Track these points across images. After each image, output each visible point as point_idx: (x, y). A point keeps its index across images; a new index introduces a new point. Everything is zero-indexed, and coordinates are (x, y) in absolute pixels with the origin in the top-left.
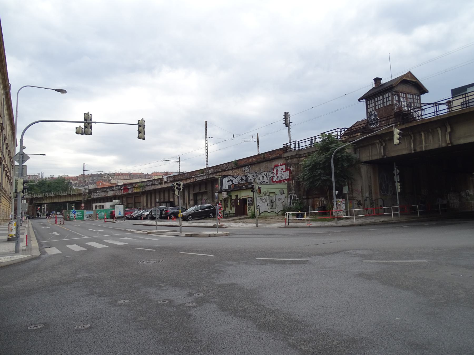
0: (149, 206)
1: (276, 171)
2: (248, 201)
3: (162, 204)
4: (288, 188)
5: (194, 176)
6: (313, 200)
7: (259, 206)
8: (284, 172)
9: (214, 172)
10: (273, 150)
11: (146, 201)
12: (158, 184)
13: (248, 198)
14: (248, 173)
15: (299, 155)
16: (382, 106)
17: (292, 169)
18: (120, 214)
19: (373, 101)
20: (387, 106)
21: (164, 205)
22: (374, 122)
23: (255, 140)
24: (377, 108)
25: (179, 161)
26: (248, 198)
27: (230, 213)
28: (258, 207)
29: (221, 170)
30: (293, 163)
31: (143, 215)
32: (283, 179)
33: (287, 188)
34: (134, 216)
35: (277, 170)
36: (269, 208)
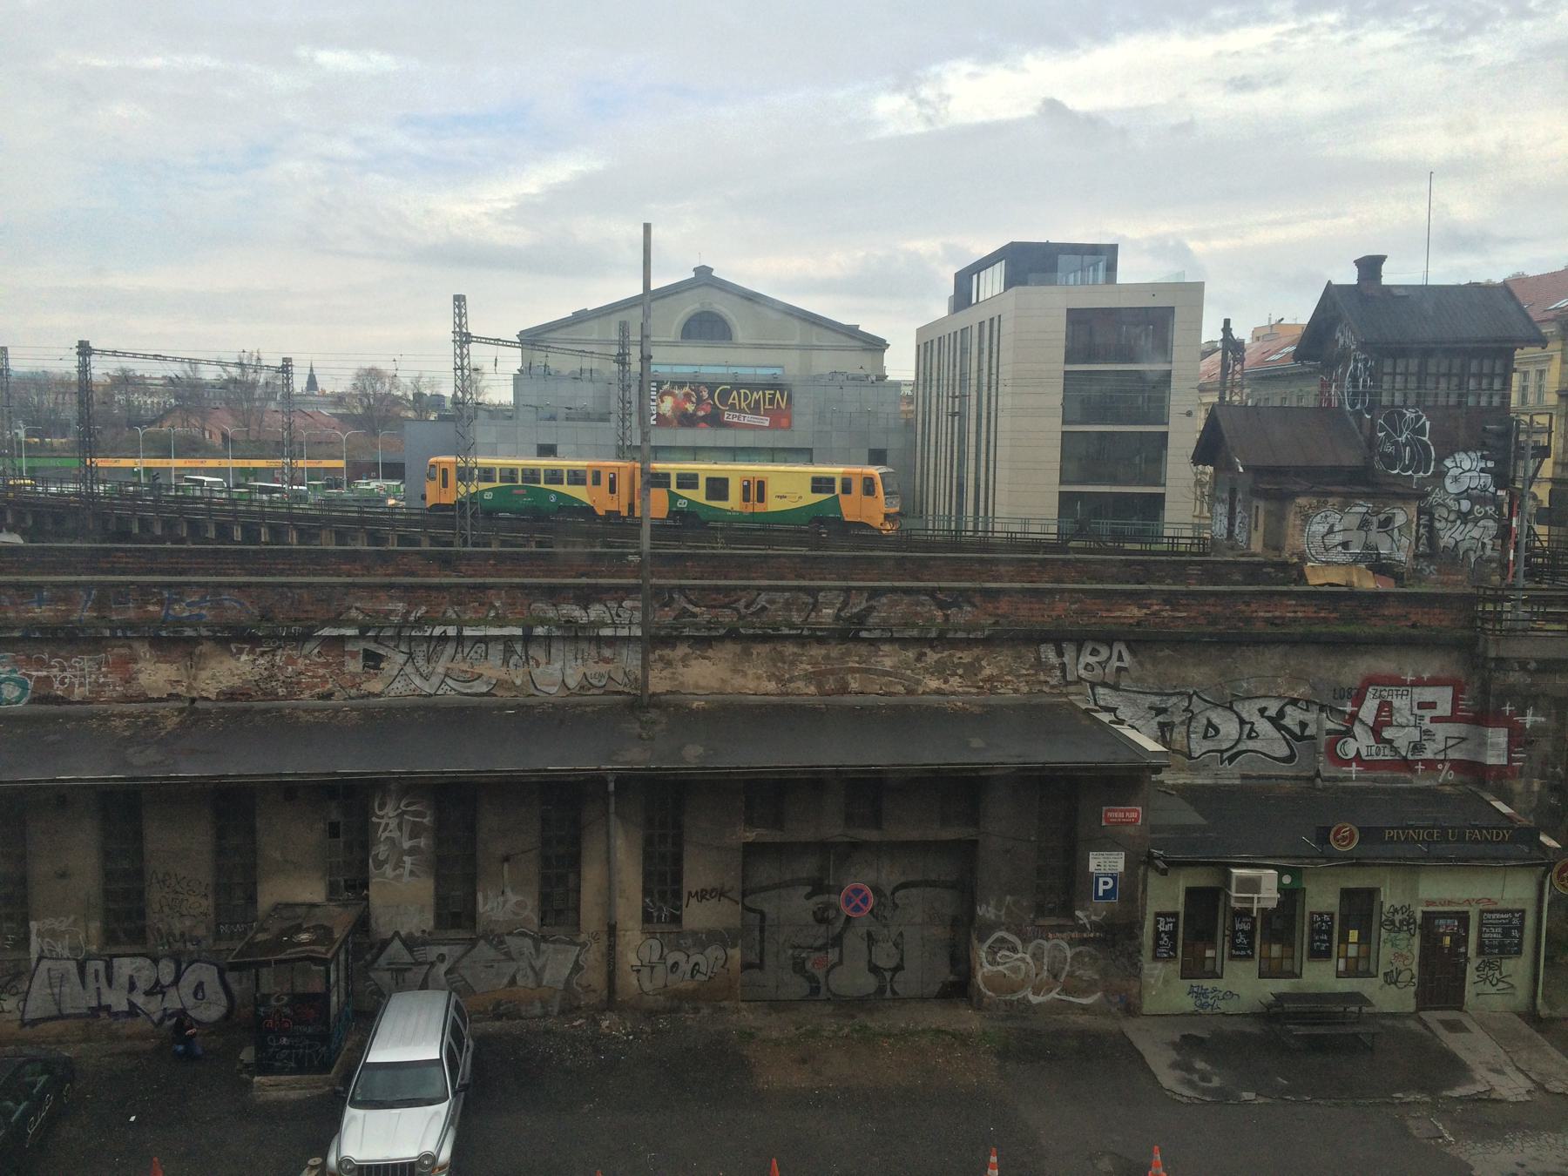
1: (1380, 709)
8: (1434, 720)
13: (1482, 912)
26: (1482, 912)
32: (1428, 755)
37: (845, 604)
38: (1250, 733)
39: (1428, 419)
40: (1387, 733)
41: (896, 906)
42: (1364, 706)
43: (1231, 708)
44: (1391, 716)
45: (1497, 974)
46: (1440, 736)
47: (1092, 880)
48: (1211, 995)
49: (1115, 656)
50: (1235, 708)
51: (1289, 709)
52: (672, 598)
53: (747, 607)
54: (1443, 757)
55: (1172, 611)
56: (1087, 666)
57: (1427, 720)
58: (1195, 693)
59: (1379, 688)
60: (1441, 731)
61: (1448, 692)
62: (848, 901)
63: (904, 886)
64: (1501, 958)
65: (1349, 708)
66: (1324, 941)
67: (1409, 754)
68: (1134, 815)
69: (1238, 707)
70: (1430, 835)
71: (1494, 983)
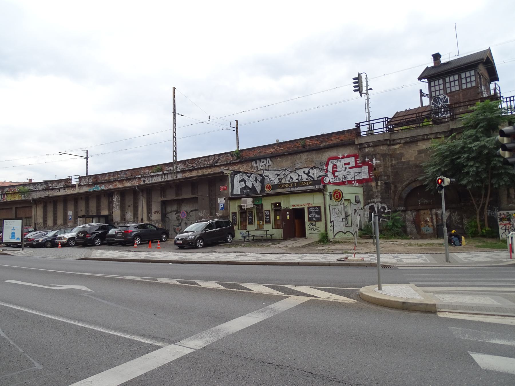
0: (50, 222)
1: (333, 167)
2: (309, 213)
3: (91, 219)
4: (365, 193)
5: (140, 176)
6: (415, 213)
7: (333, 221)
9: (187, 169)
10: (324, 133)
11: (42, 216)
12: (59, 189)
13: (308, 208)
14: (266, 170)
15: (390, 141)
16: (457, 88)
17: (374, 162)
18: (13, 237)
19: (441, 81)
20: (467, 89)
21: (94, 221)
22: (443, 110)
23: (234, 129)
24: (448, 91)
25: (86, 156)
26: (308, 208)
27: (267, 235)
28: (332, 223)
29: (202, 166)
30: (378, 154)
31: (60, 238)
32: (349, 179)
33: (362, 193)
34: (38, 241)
35: (335, 166)
36: (345, 226)
37: (214, 159)
38: (301, 179)
39: (448, 96)
40: (336, 174)
41: (190, 216)
42: (329, 167)
43: (296, 172)
44: (337, 169)
45: (315, 227)
46: (352, 173)
47: (219, 205)
48: (245, 235)
49: (268, 162)
50: (297, 172)
51: (311, 171)
52: (186, 163)
53: (198, 163)
54: (354, 179)
55: (279, 148)
56: (262, 166)
57: (348, 168)
58: (286, 169)
59: (332, 161)
60: (352, 171)
61: (353, 159)
62: (182, 215)
63: (191, 211)
64: (315, 222)
65: (325, 168)
66: (268, 218)
67: (343, 179)
68: (225, 188)
69: (298, 171)
70: (290, 185)
71: (314, 230)
